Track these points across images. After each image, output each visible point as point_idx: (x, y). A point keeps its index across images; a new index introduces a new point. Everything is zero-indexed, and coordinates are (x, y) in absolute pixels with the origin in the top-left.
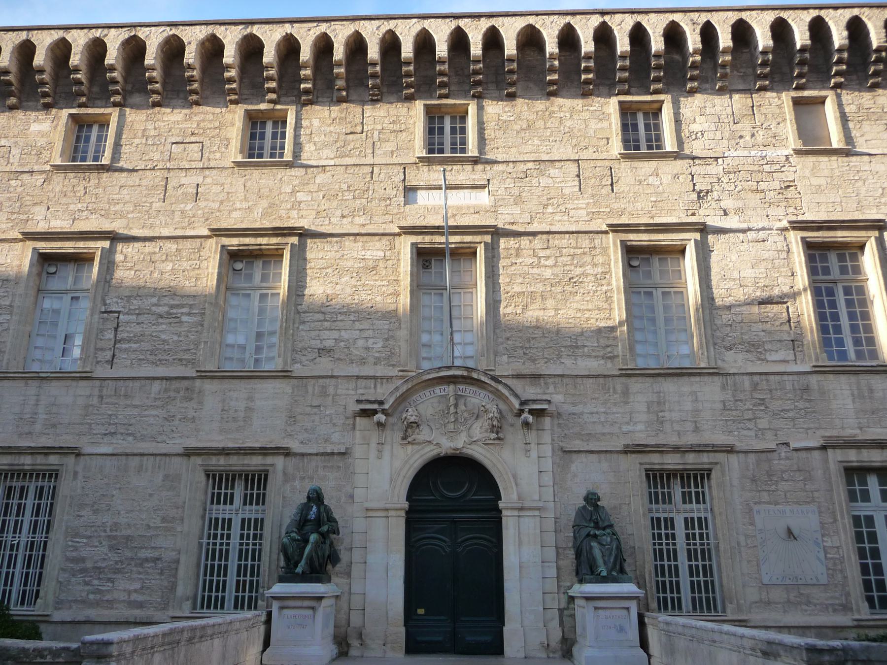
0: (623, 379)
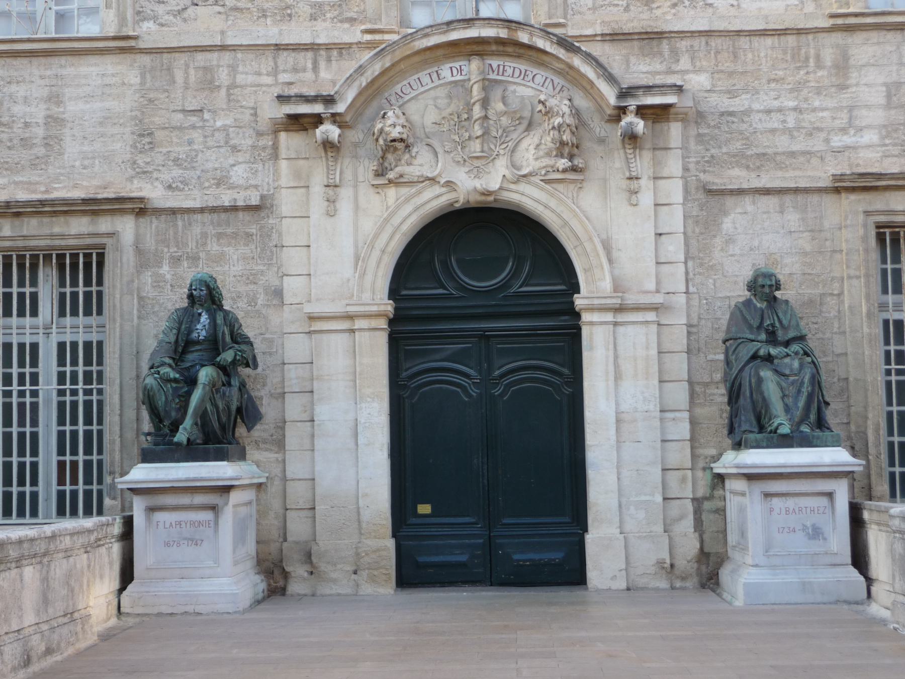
0: (838, 38)
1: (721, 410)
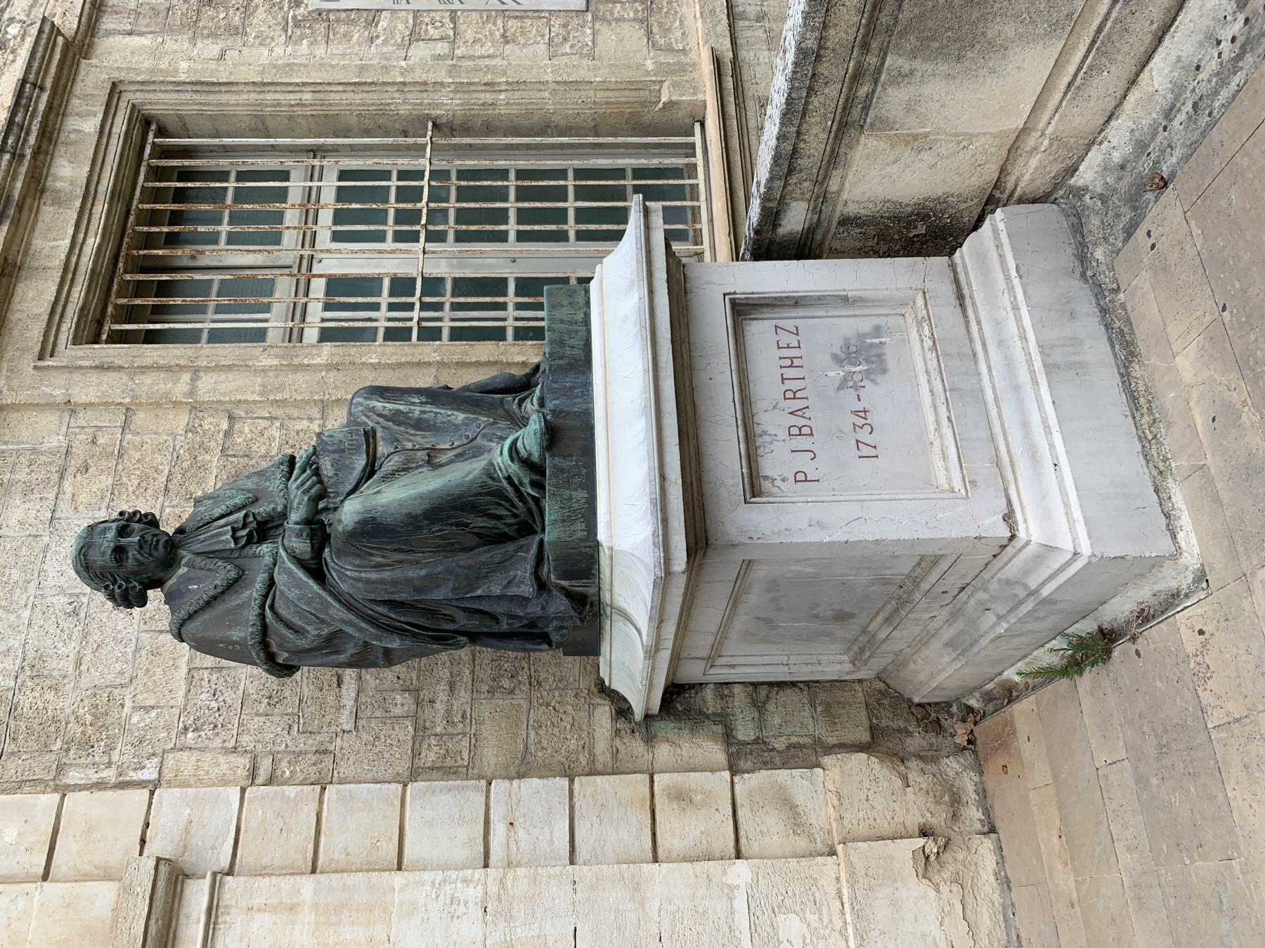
1: (491, 691)
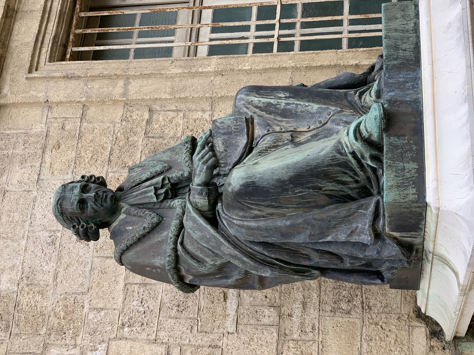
1: (333, 311)
